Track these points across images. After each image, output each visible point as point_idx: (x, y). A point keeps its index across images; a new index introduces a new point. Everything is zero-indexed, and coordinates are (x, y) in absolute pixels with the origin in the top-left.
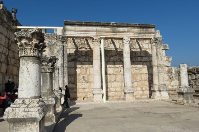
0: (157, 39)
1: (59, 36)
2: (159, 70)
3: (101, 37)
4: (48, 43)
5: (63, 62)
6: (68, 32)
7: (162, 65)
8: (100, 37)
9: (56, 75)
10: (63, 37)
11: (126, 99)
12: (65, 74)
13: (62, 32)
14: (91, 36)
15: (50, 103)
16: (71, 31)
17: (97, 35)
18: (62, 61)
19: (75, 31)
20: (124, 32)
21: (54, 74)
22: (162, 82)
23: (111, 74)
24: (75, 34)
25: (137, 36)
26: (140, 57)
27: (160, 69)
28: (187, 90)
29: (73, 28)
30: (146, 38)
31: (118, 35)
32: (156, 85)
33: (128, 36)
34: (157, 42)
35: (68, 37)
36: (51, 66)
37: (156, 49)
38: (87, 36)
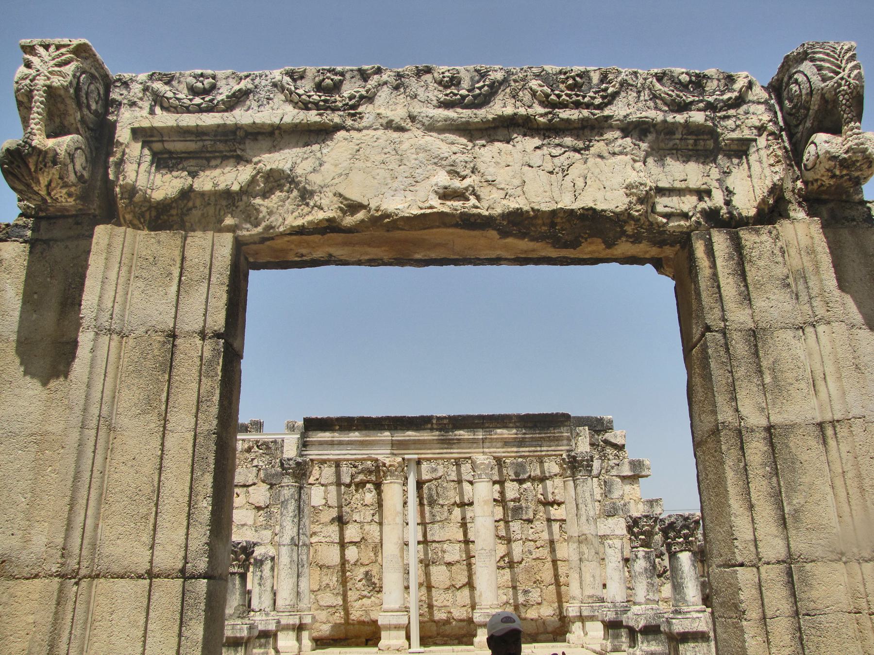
0: (574, 457)
1: (289, 460)
2: (583, 553)
3: (406, 457)
4: (266, 469)
5: (295, 534)
6: (314, 447)
7: (589, 536)
8: (403, 459)
9: (264, 573)
10: (298, 464)
11: (475, 644)
12: (303, 566)
13: (298, 447)
14: (376, 456)
15: (238, 635)
16: (321, 443)
17: (395, 452)
18: (295, 530)
19: (332, 444)
20: (474, 442)
21: (261, 571)
22: (589, 591)
23: (453, 565)
24: (332, 452)
25: (515, 449)
26: (552, 504)
27: (584, 548)
28: (617, 614)
29: (326, 436)
30: (543, 453)
31: (455, 451)
32: (574, 598)
33: (486, 450)
34: (575, 467)
35: (312, 460)
36: (245, 561)
37: (575, 488)
38: (365, 456)
